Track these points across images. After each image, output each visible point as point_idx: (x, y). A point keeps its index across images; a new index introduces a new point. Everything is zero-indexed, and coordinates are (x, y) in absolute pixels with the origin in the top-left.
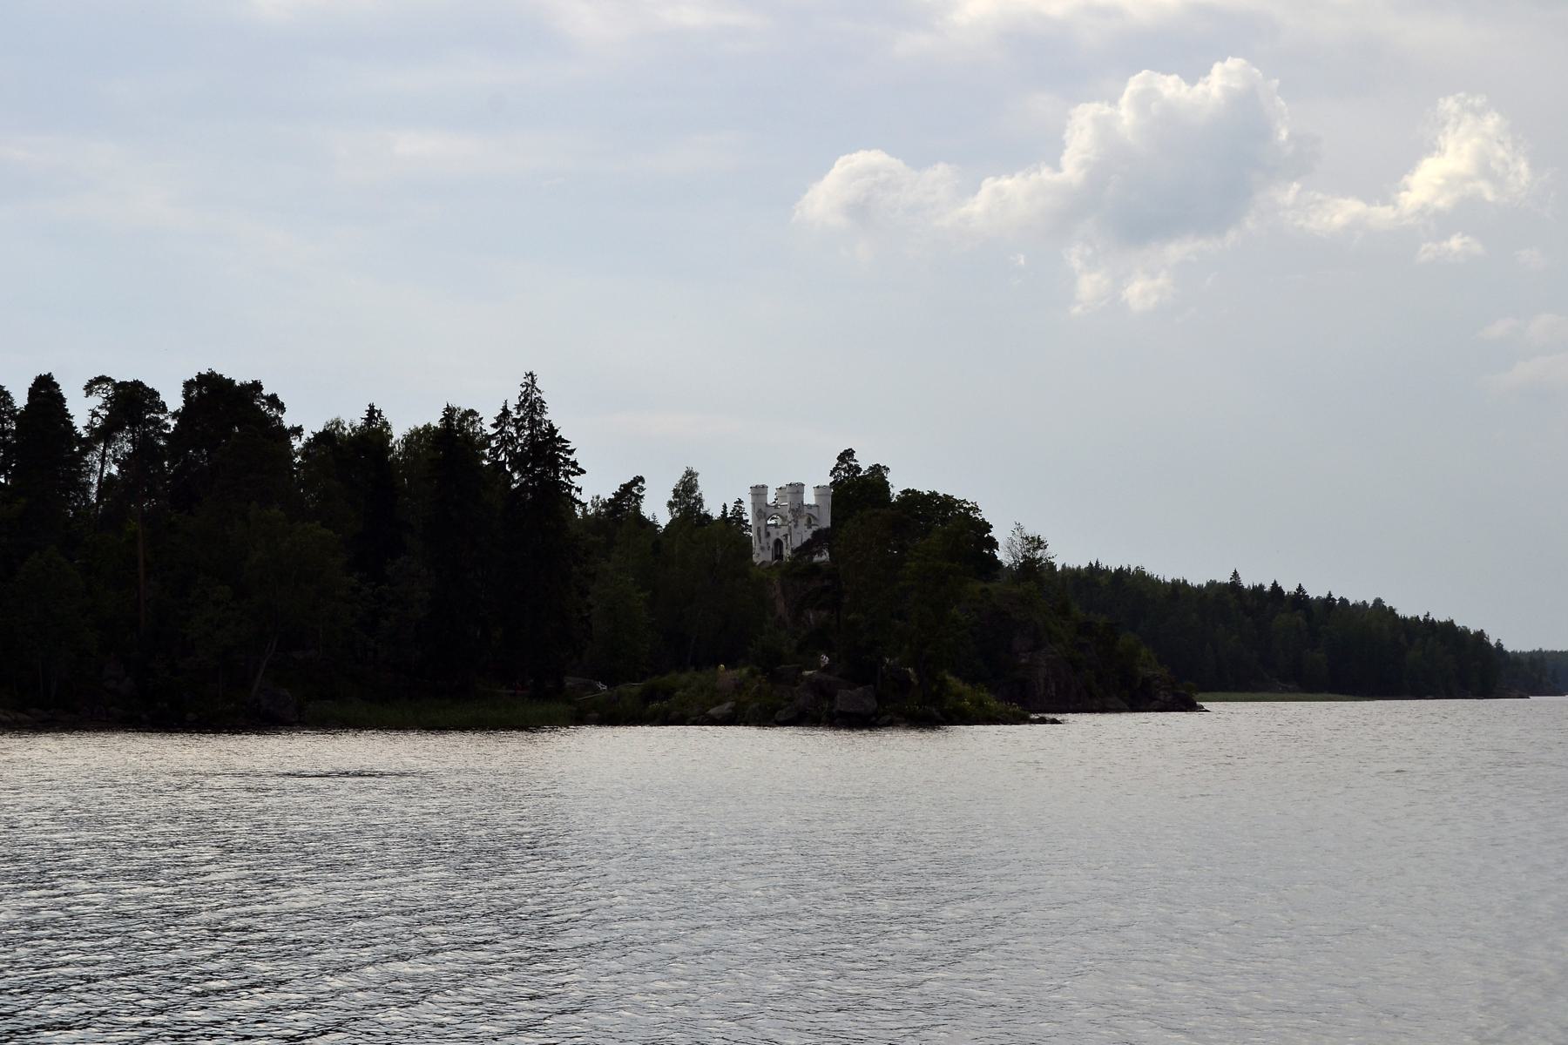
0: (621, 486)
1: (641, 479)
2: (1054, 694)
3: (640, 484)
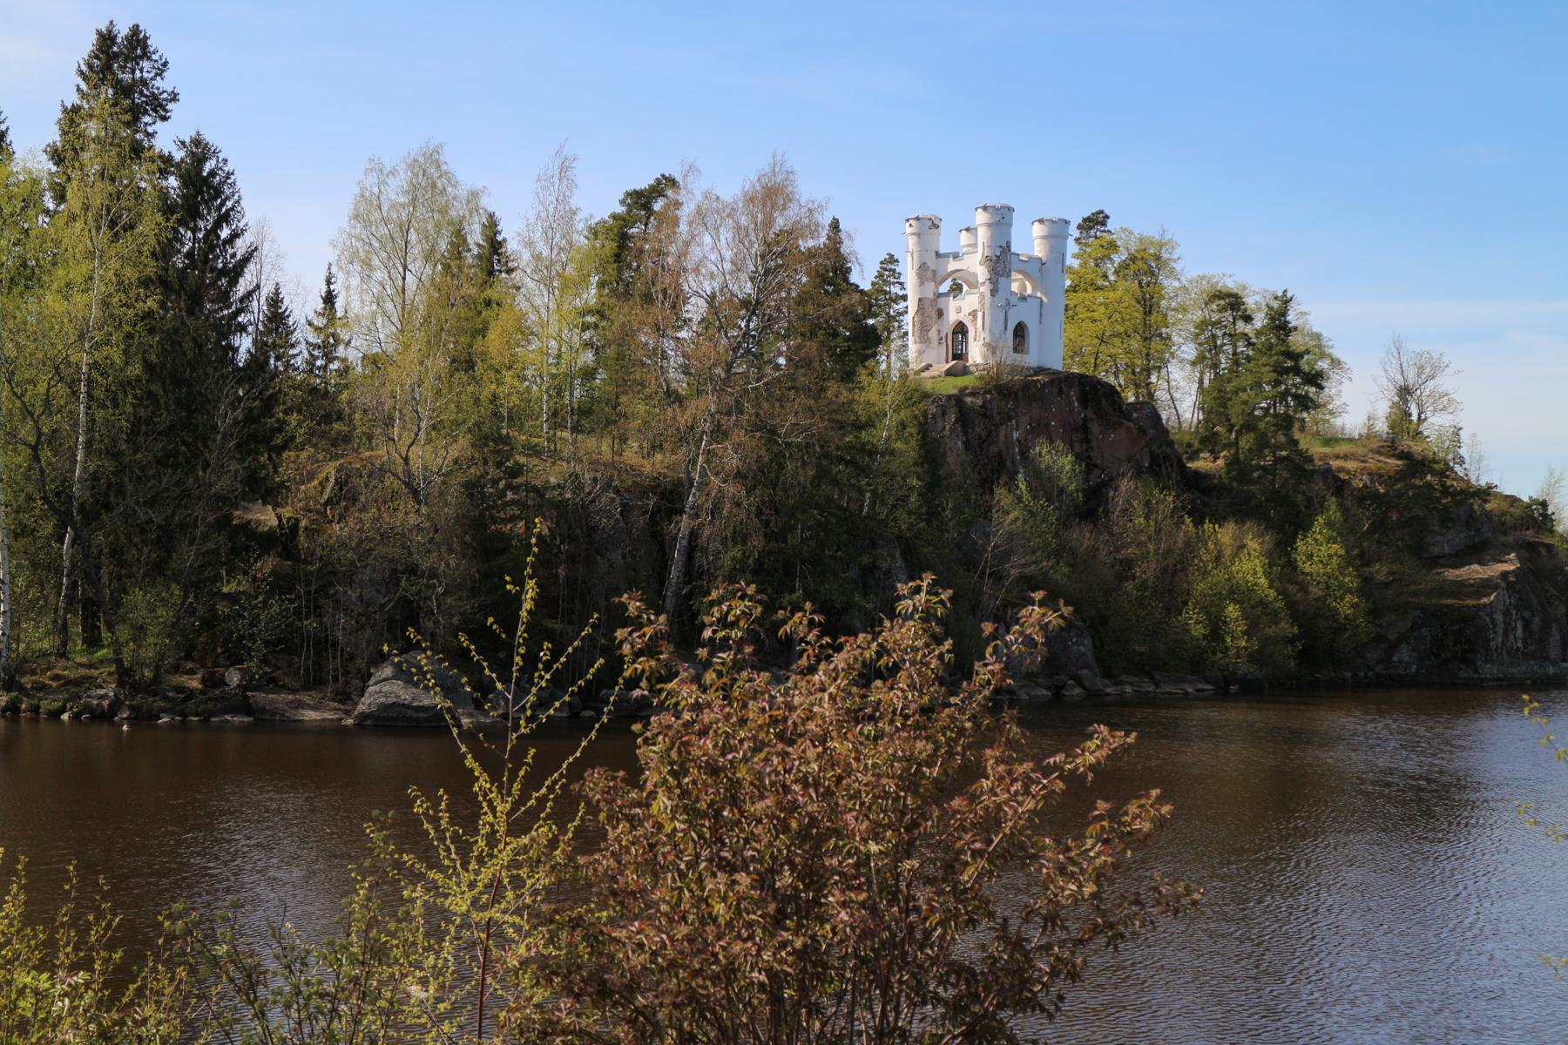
0: (628, 194)
1: (672, 182)
2: (1520, 645)
3: (670, 193)
